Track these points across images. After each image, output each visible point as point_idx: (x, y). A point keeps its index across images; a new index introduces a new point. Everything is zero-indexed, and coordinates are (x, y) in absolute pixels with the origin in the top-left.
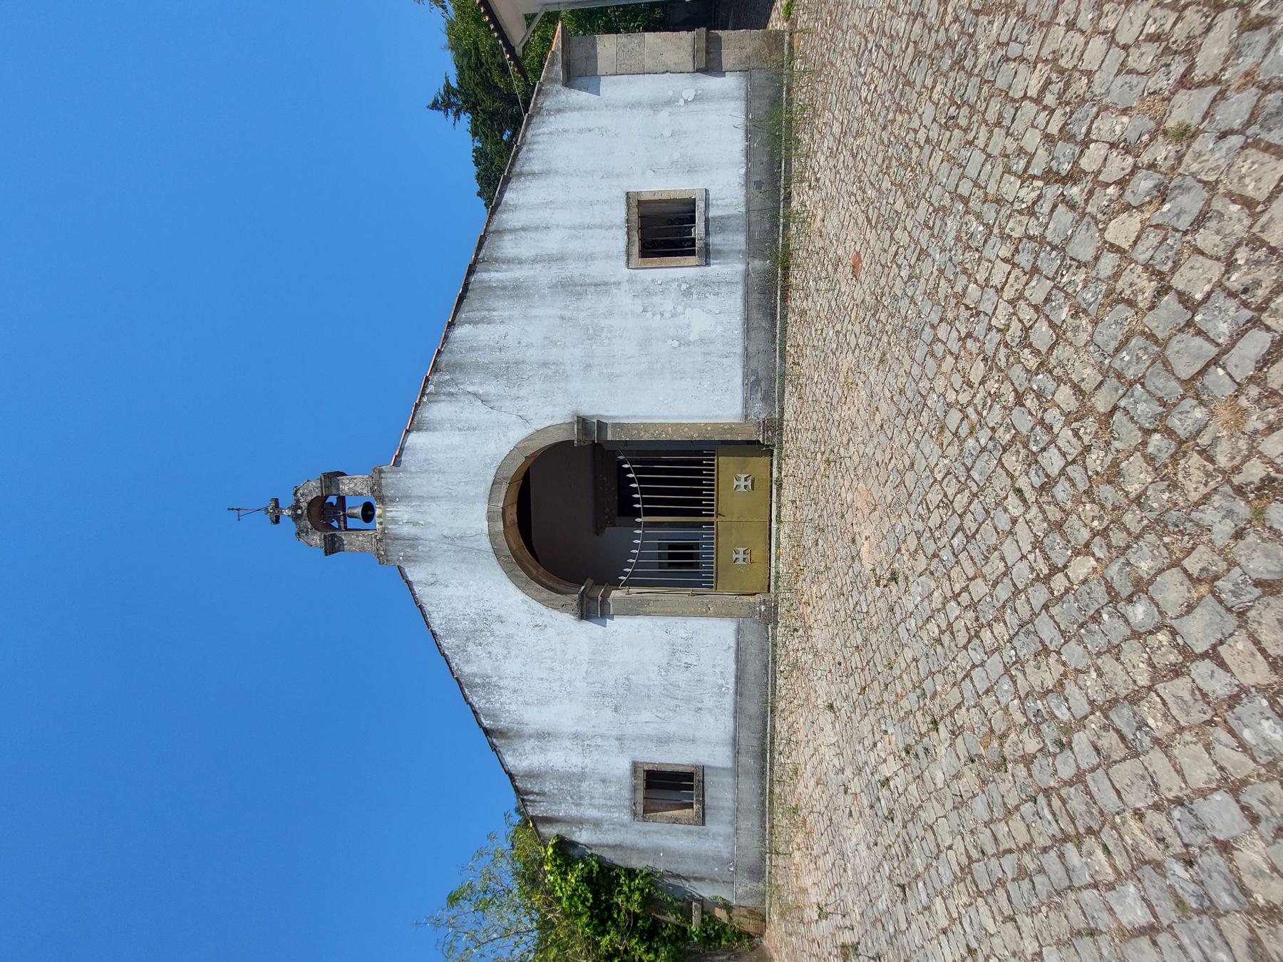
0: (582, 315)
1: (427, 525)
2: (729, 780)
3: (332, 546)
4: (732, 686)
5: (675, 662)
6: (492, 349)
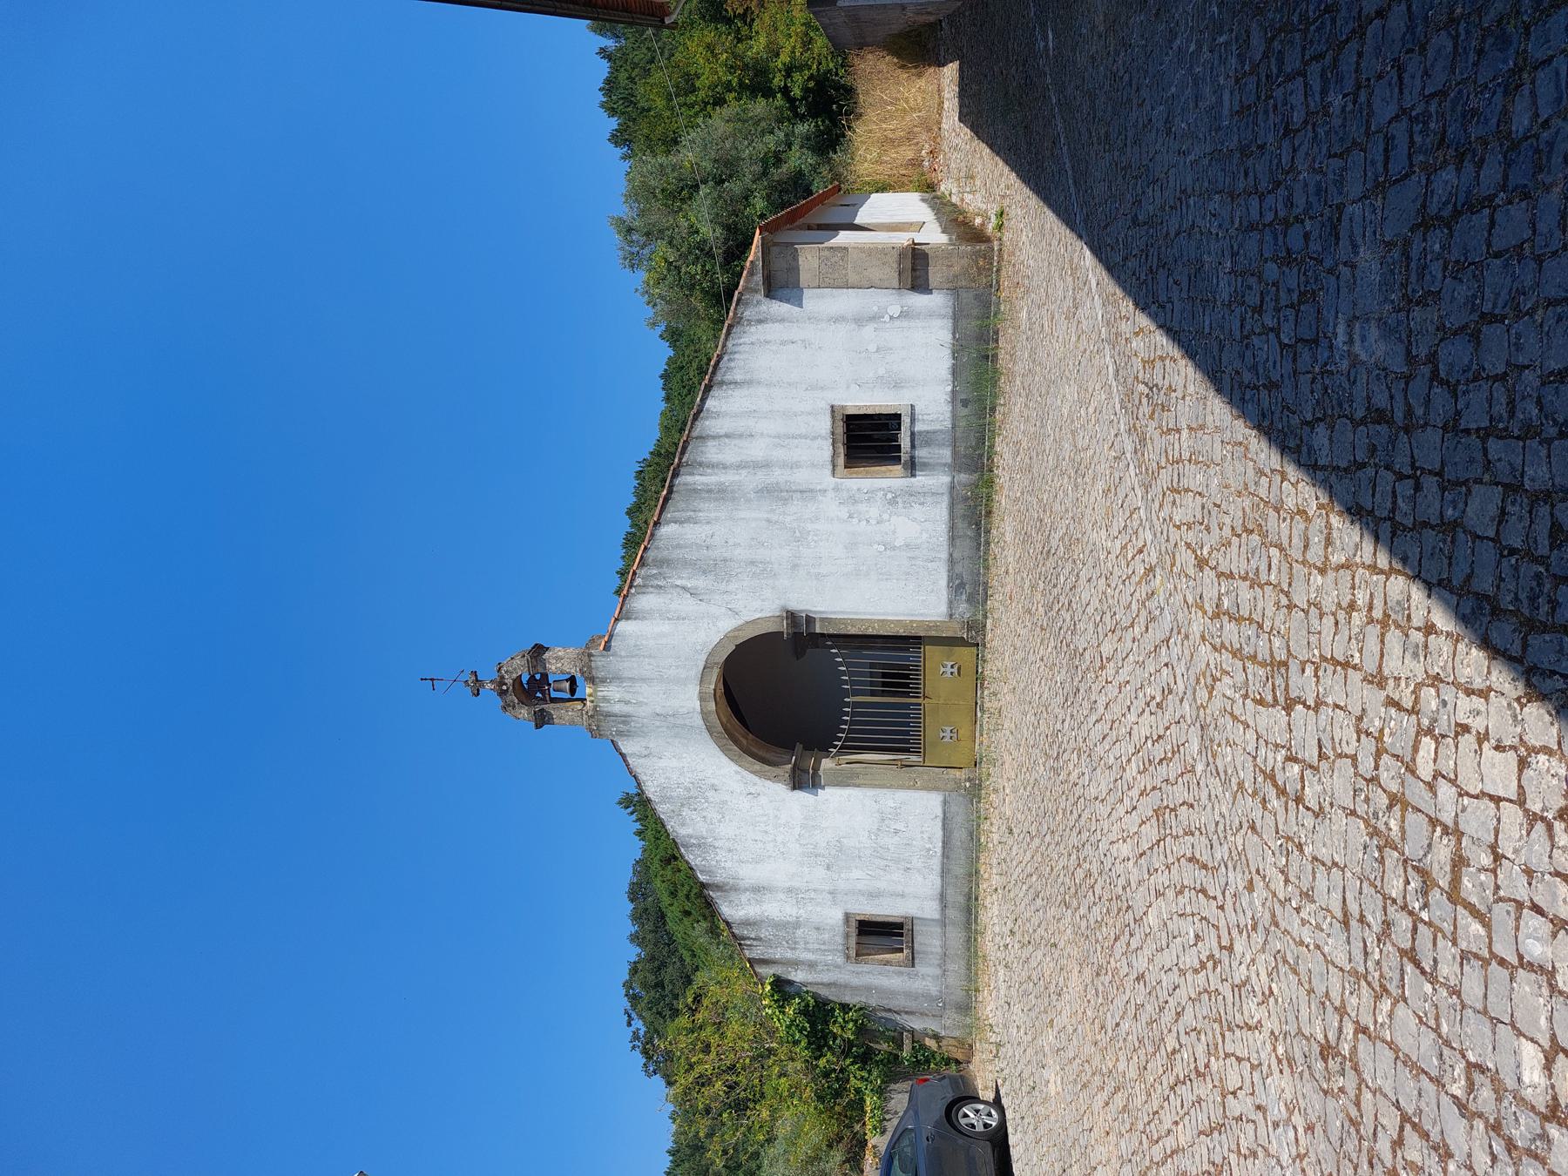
0: (788, 519)
1: (640, 704)
4: (939, 850)
6: (699, 547)
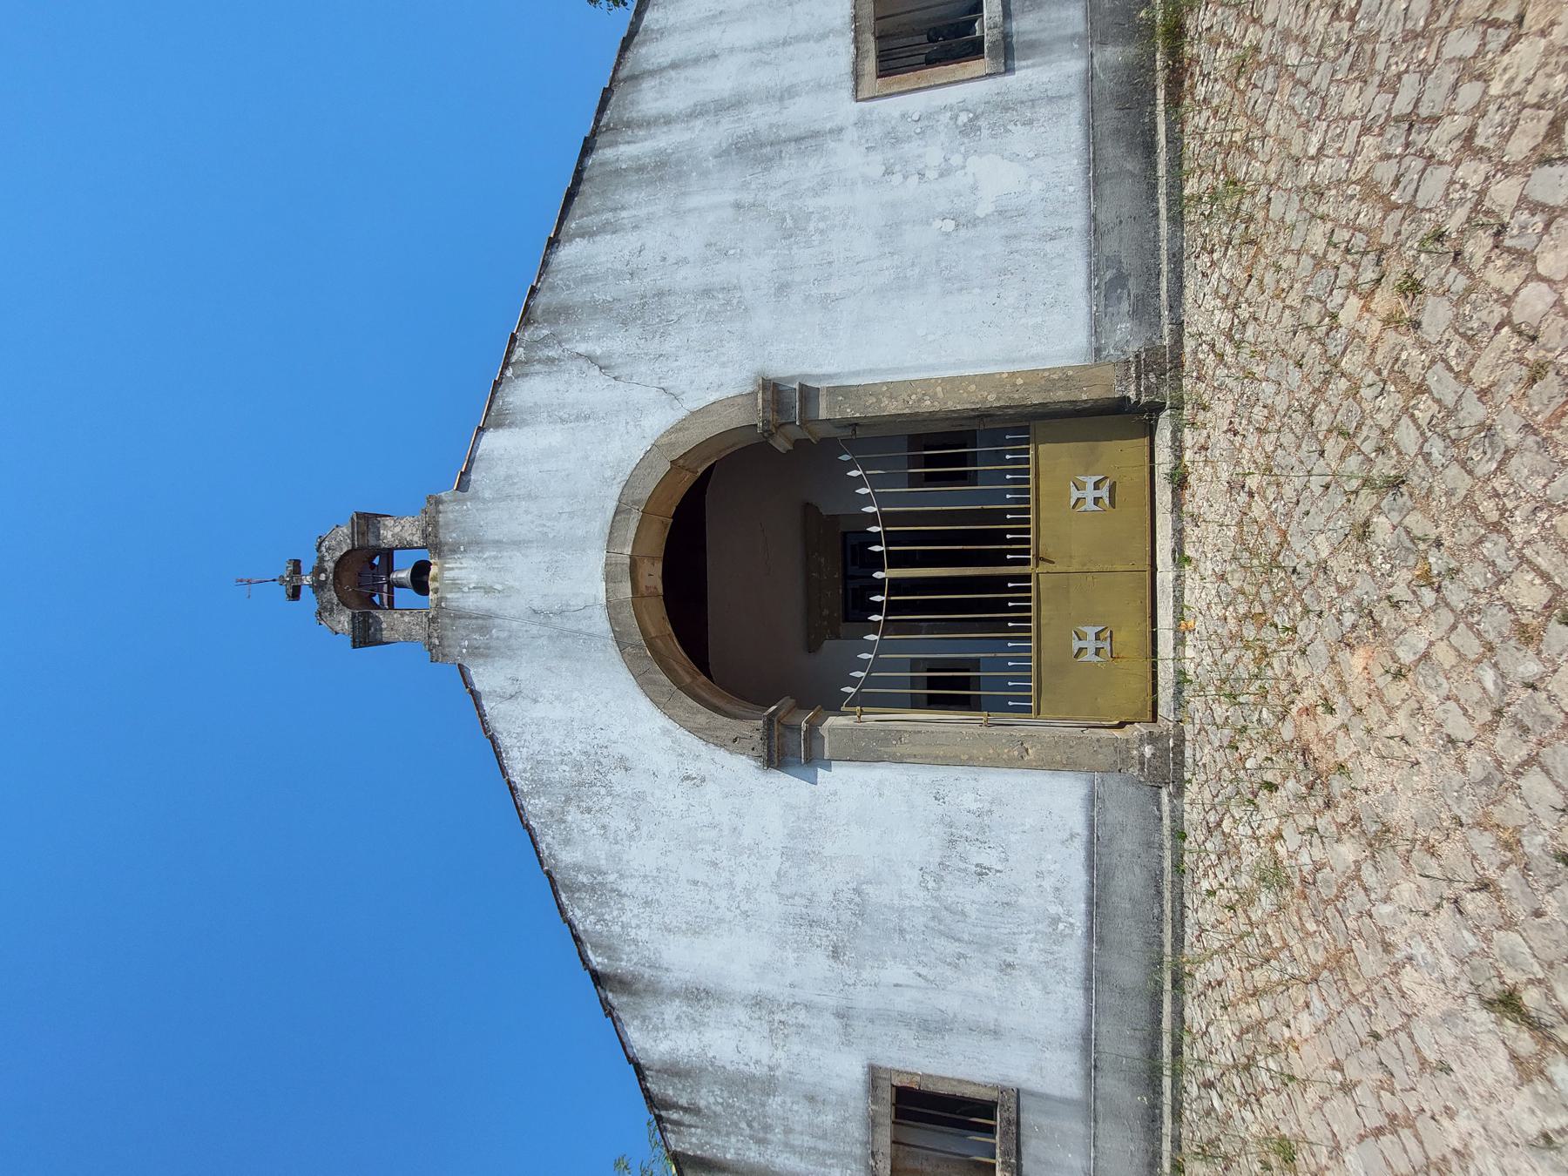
0: (774, 195)
1: (507, 592)
2: (1075, 1127)
3: (365, 635)
4: (1079, 920)
5: (955, 862)
6: (618, 275)
